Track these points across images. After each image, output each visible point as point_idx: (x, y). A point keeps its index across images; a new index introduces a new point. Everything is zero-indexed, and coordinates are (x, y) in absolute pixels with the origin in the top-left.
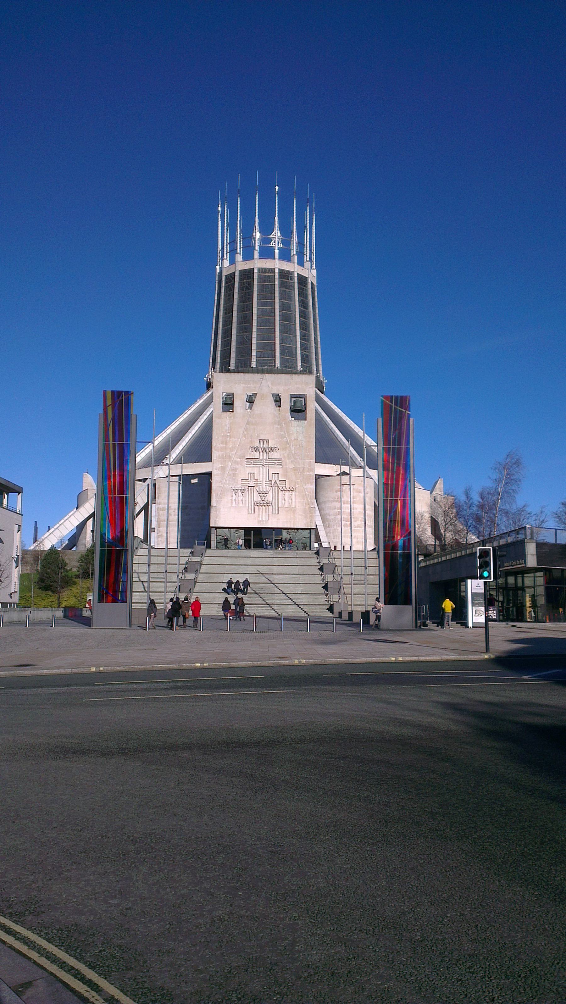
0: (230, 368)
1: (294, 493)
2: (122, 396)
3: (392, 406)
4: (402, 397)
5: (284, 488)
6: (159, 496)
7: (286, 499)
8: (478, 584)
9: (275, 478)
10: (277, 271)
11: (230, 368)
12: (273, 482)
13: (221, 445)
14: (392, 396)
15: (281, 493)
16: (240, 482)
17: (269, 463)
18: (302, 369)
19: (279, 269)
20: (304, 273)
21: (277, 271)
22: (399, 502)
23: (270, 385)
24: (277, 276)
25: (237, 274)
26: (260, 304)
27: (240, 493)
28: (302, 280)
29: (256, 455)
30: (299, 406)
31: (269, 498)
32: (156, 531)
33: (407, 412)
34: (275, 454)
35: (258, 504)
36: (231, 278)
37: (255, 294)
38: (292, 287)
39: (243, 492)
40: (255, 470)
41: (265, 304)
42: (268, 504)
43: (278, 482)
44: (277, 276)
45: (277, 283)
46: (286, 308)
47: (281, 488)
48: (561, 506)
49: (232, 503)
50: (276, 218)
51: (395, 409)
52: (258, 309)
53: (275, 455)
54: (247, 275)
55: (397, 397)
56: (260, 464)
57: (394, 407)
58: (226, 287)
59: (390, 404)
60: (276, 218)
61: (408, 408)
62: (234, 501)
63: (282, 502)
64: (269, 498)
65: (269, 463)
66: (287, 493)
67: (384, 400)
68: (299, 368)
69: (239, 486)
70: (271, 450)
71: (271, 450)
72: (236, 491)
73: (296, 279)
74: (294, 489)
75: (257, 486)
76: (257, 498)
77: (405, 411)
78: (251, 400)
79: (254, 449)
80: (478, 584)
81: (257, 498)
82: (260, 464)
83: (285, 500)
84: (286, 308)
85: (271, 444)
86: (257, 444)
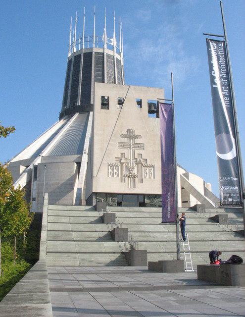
5: (146, 164)
6: (39, 176)
7: (148, 172)
13: (100, 132)
16: (115, 159)
20: (119, 58)
21: (105, 54)
26: (96, 70)
28: (119, 62)
29: (125, 140)
30: (153, 108)
32: (36, 200)
34: (139, 139)
36: (77, 58)
37: (93, 65)
40: (125, 151)
41: (98, 71)
42: (134, 177)
43: (141, 160)
45: (105, 60)
49: (108, 174)
50: (105, 29)
54: (88, 56)
60: (105, 29)
62: (110, 175)
63: (145, 175)
64: (135, 171)
70: (137, 137)
71: (137, 137)
76: (126, 172)
78: (121, 102)
79: (123, 136)
81: (126, 172)
83: (146, 173)
85: (136, 133)
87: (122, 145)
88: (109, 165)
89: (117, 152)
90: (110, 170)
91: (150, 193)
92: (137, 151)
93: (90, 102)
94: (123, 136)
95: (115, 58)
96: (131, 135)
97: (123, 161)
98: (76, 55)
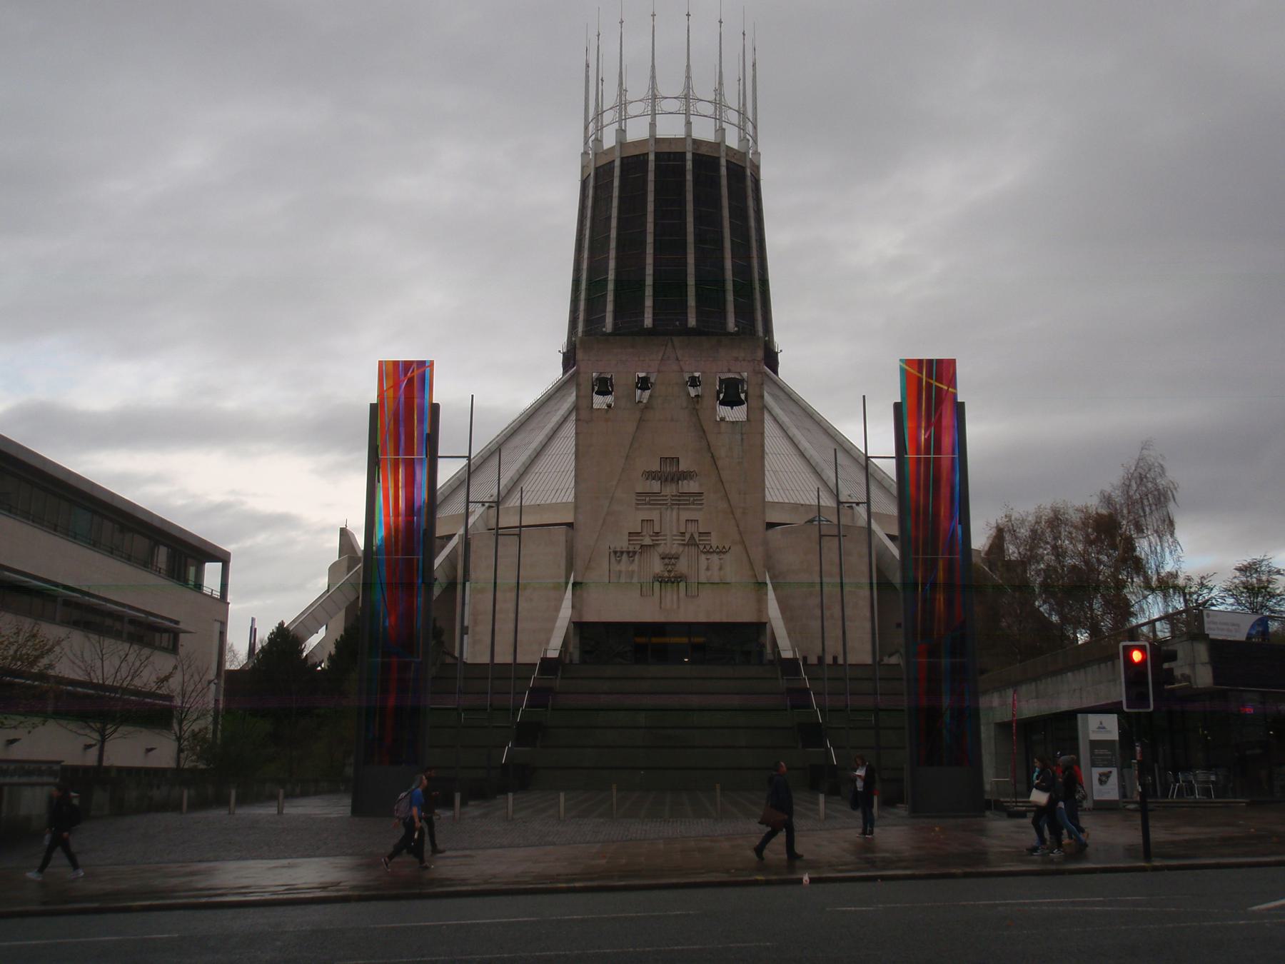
0: (604, 329)
1: (727, 557)
2: (413, 371)
3: (922, 379)
4: (940, 362)
5: (708, 547)
8: (1101, 723)
9: (692, 528)
10: (689, 156)
11: (604, 329)
12: (687, 536)
14: (920, 362)
15: (703, 557)
16: (626, 537)
17: (679, 500)
18: (736, 329)
19: (693, 153)
21: (689, 156)
22: (941, 564)
23: (680, 358)
24: (689, 165)
25: (617, 163)
27: (625, 556)
29: (655, 486)
31: (682, 566)
32: (469, 632)
33: (950, 389)
34: (692, 483)
35: (662, 580)
37: (651, 198)
38: (716, 183)
39: (631, 554)
40: (654, 515)
43: (697, 539)
44: (689, 165)
45: (689, 177)
46: (707, 220)
47: (701, 547)
48: (1238, 574)
51: (929, 385)
52: (656, 225)
53: (691, 486)
55: (930, 362)
56: (663, 504)
57: (926, 381)
58: (596, 188)
59: (920, 375)
61: (952, 382)
65: (679, 500)
66: (715, 558)
67: (907, 368)
68: (731, 325)
69: (623, 543)
70: (687, 476)
71: (687, 476)
72: (618, 554)
73: (723, 171)
74: (727, 548)
75: (657, 544)
76: (657, 567)
77: (946, 388)
79: (650, 475)
80: (1101, 723)
82: (663, 504)
84: (707, 220)
85: (683, 467)
86: (655, 467)
87: (645, 499)
88: (615, 552)
89: (633, 519)
90: (615, 567)
91: (717, 620)
92: (685, 515)
93: (643, 321)
94: (650, 475)
95: (723, 162)
96: (670, 473)
97: (647, 541)
98: (600, 163)
